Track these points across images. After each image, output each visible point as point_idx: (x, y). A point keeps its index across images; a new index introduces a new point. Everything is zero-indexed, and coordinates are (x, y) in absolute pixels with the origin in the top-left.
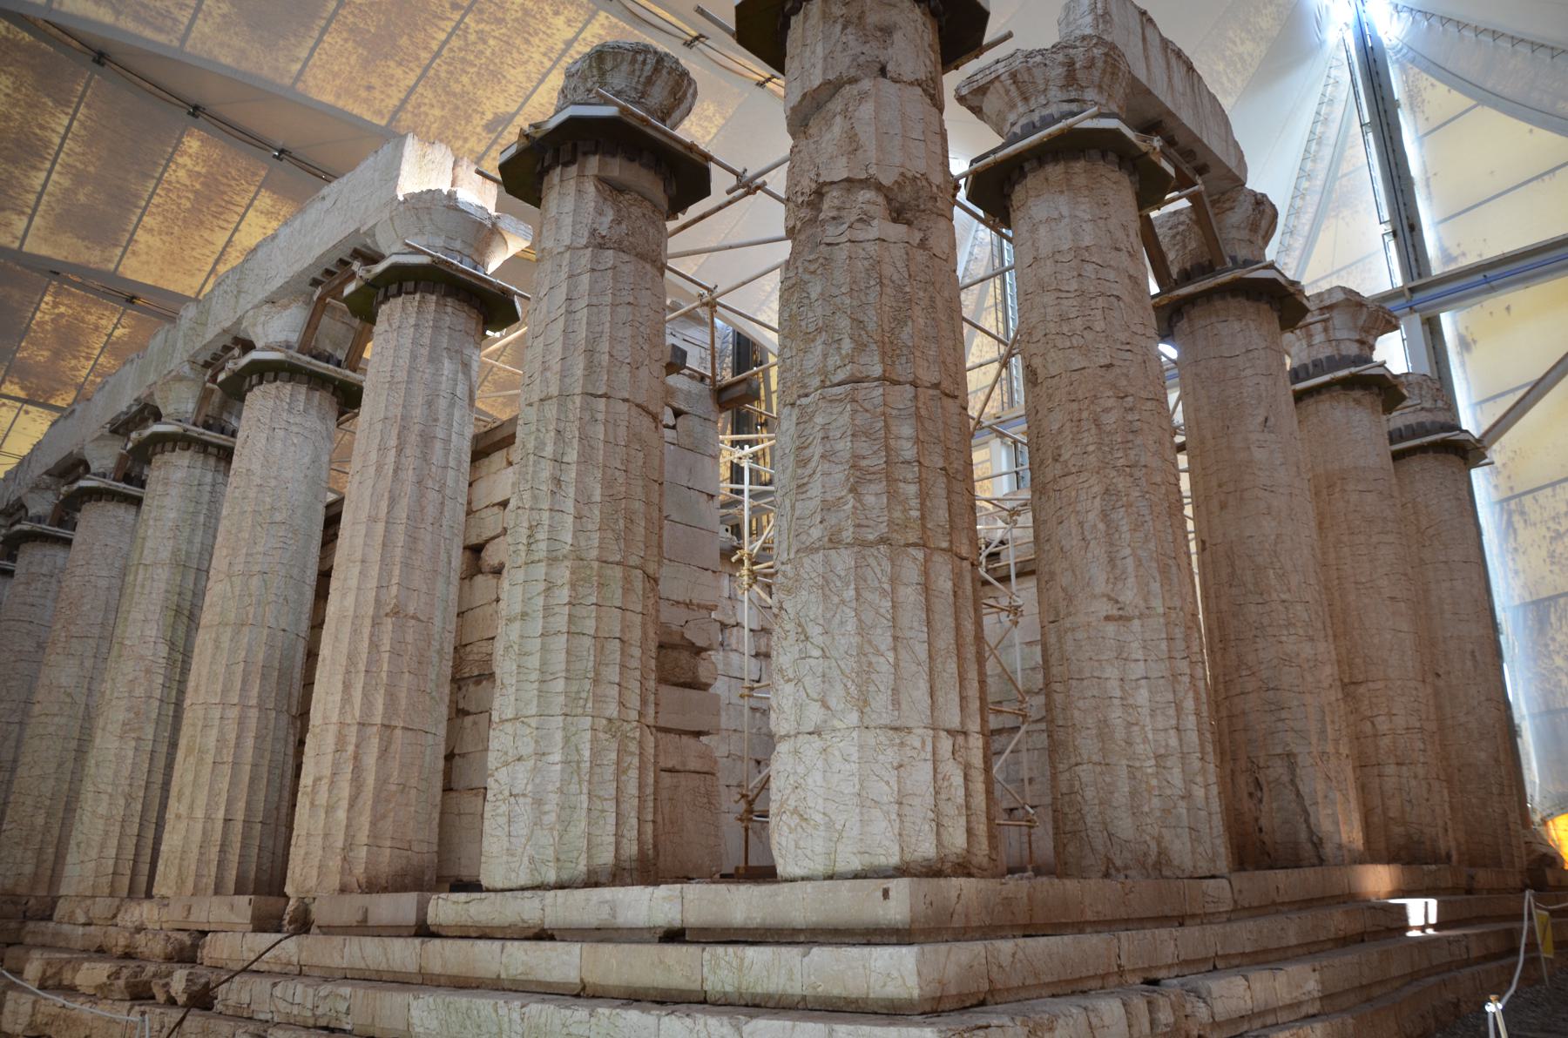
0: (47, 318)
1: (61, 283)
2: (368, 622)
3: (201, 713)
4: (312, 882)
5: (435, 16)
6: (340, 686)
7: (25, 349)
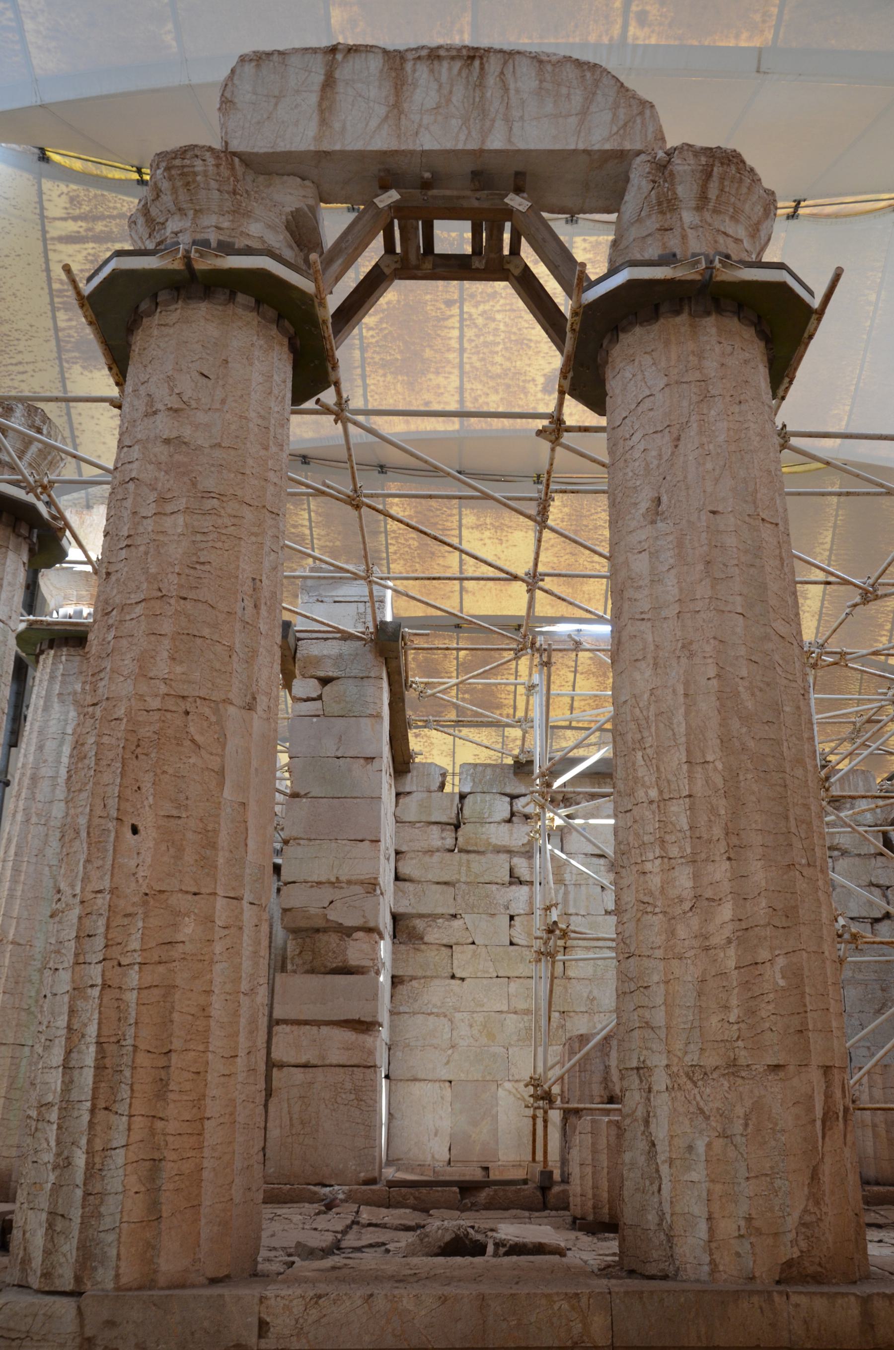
5: (439, 320)
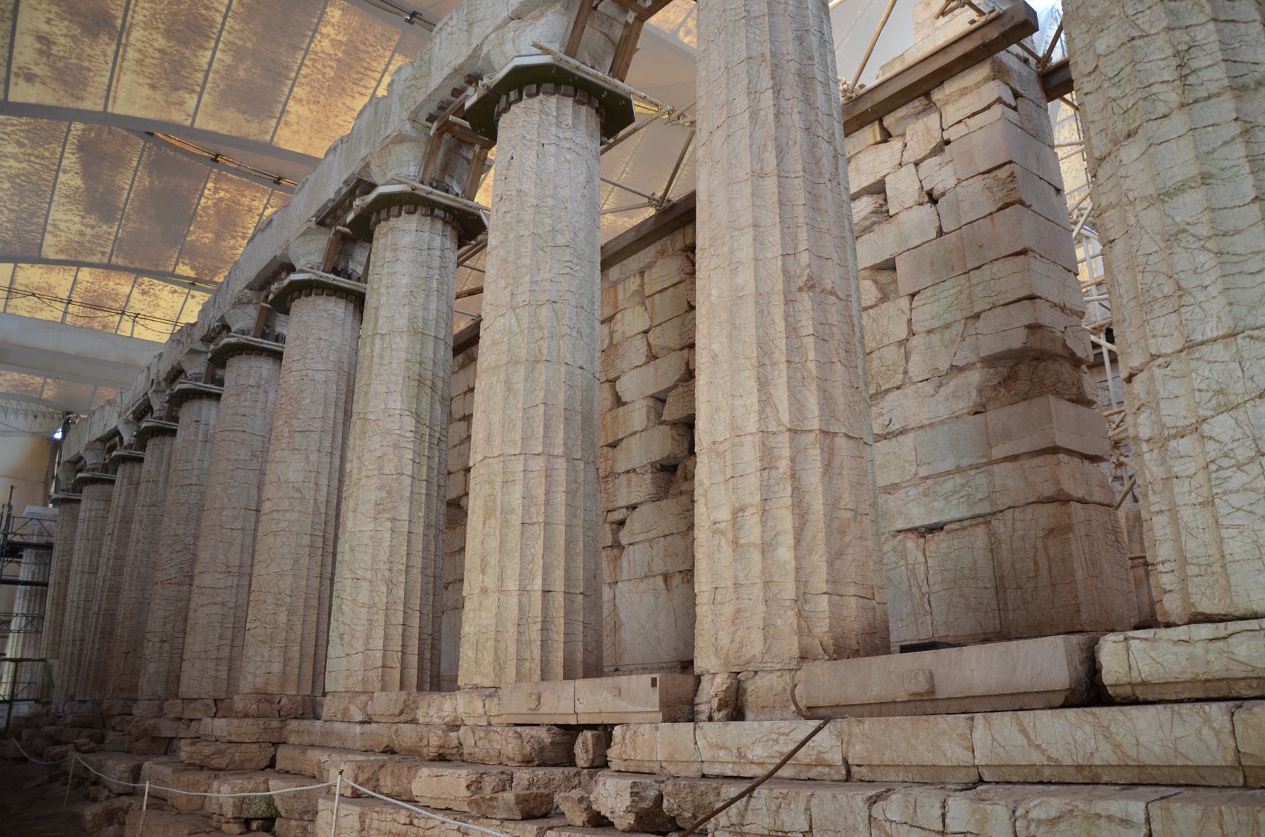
0: (210, 203)
1: (220, 170)
2: (778, 299)
3: (497, 466)
4: (756, 646)
6: (753, 384)
7: (193, 233)
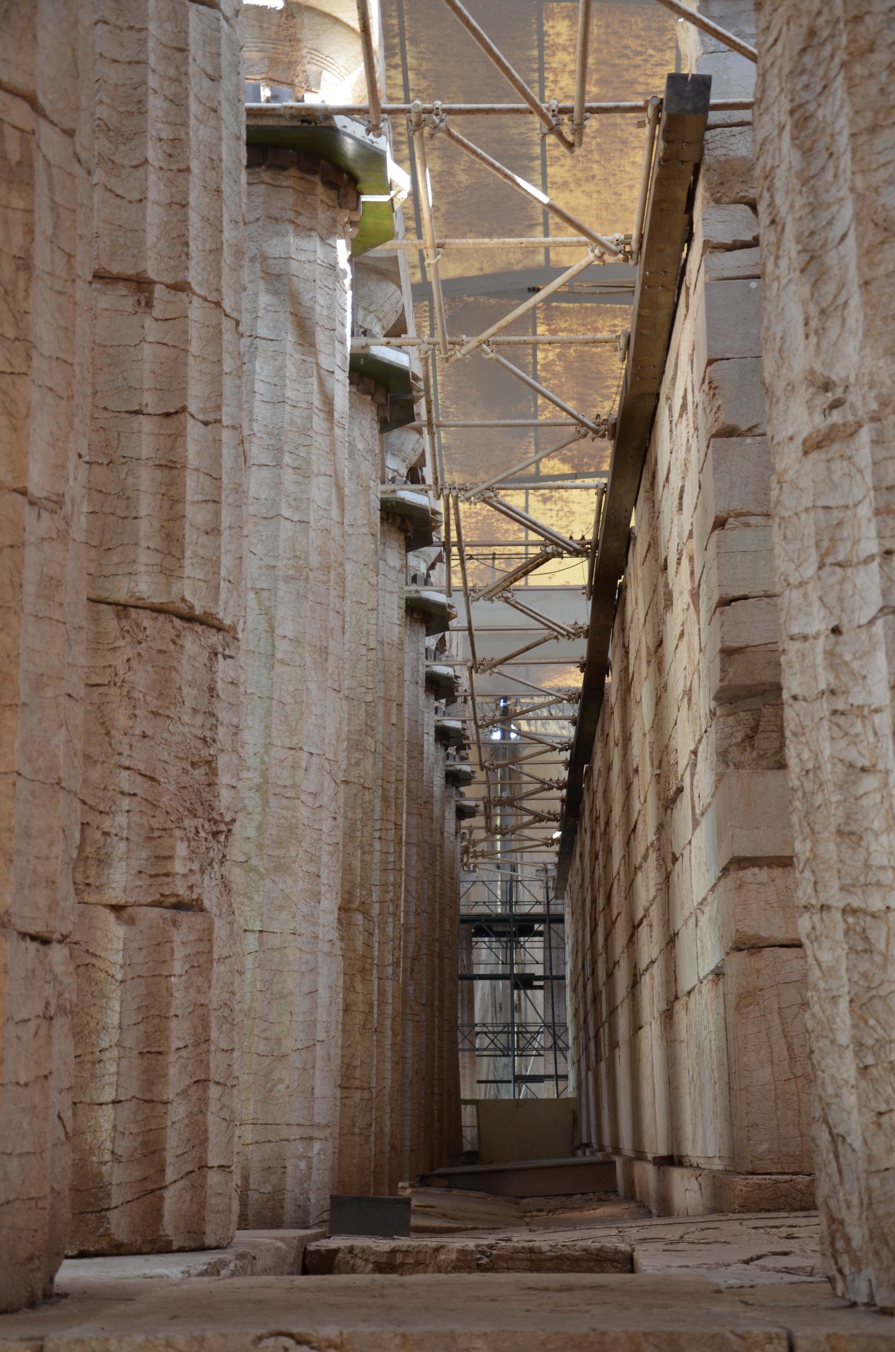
0: (551, 356)
